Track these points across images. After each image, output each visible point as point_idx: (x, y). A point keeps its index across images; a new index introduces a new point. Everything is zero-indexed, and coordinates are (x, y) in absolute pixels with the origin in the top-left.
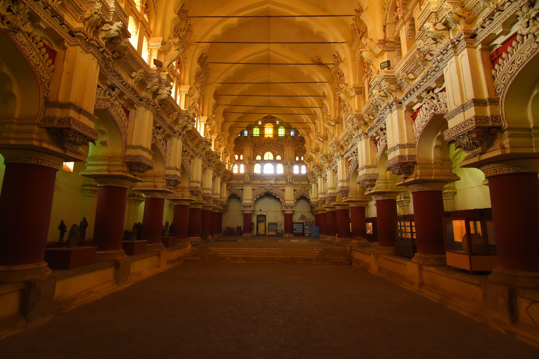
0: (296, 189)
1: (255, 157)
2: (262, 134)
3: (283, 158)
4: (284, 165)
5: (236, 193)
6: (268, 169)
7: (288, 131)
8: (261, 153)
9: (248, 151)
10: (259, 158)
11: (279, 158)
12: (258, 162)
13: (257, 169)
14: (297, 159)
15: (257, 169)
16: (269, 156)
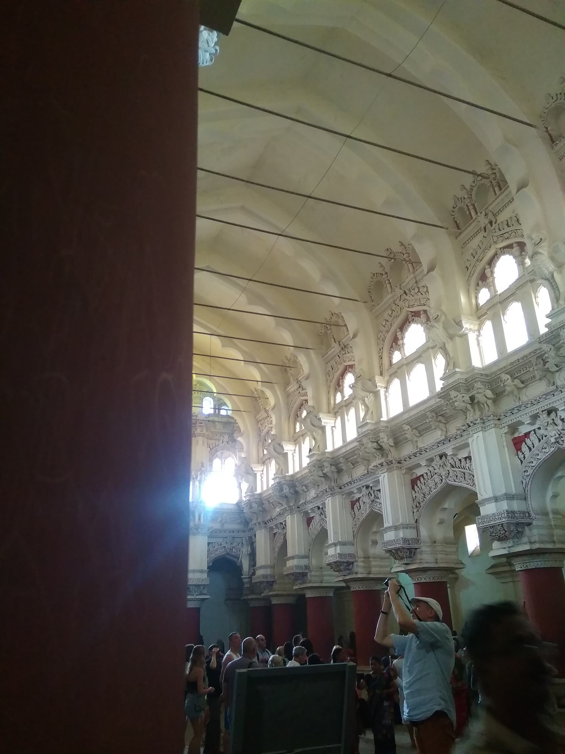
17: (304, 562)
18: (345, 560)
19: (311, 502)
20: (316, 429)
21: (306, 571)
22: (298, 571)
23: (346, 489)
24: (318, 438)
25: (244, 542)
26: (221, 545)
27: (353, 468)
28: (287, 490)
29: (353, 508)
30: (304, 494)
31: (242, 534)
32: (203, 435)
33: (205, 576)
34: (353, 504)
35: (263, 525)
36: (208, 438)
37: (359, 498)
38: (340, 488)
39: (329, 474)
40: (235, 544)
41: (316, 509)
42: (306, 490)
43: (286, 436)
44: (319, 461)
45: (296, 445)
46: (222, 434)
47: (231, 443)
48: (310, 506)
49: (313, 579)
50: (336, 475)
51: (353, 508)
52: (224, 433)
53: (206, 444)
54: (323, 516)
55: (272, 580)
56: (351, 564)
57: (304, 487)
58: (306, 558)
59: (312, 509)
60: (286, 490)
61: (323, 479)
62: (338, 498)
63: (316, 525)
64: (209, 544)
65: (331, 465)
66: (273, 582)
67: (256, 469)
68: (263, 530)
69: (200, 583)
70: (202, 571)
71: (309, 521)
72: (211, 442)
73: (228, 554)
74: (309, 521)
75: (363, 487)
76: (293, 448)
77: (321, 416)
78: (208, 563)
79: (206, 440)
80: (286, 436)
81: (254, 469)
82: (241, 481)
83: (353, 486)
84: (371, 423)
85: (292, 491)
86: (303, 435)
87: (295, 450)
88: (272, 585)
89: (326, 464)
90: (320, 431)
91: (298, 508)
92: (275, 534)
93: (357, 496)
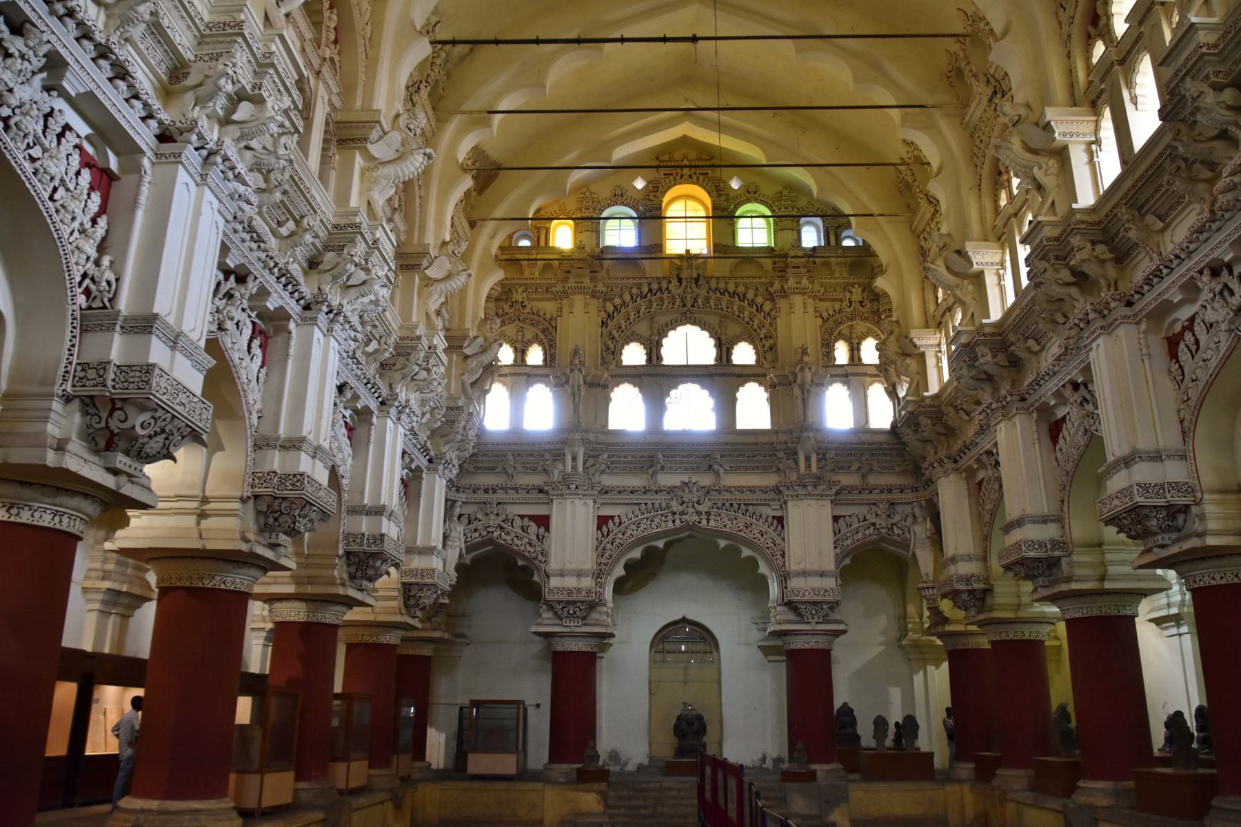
0: (838, 513)
1: (616, 354)
2: (652, 247)
3: (766, 350)
4: (771, 388)
5: (516, 539)
6: (691, 412)
7: (787, 223)
8: (643, 328)
9: (580, 322)
10: (634, 355)
11: (744, 354)
12: (634, 375)
13: (626, 411)
14: (841, 353)
15: (626, 411)
16: (689, 344)
17: (1049, 532)
18: (1160, 502)
19: (1051, 374)
20: (1042, 160)
21: (1057, 553)
22: (1031, 554)
23: (1149, 300)
24: (1049, 182)
25: (917, 512)
26: (865, 520)
27: (1162, 231)
28: (989, 358)
29: (1174, 355)
30: (1034, 359)
31: (909, 496)
32: (803, 291)
33: (830, 583)
34: (1173, 344)
35: (949, 465)
36: (814, 298)
37: (1192, 320)
38: (1130, 304)
39: (1091, 269)
40: (897, 518)
41: (1068, 392)
42: (1036, 348)
43: (975, 228)
44: (1057, 239)
45: (1003, 248)
46: (847, 287)
47: (869, 305)
48: (1052, 386)
49: (1078, 572)
50: (1111, 271)
51: (1174, 355)
52: (852, 285)
53: (811, 309)
54: (1090, 407)
55: (981, 586)
56: (1179, 511)
57: (1031, 343)
58: (1052, 521)
59: (1058, 394)
60: (986, 358)
61: (1074, 291)
62: (1127, 336)
63: (1071, 436)
64: (836, 519)
65: (1093, 243)
66: (984, 591)
67: (923, 342)
68: (951, 477)
69: (819, 598)
70: (822, 574)
71: (1055, 430)
72: (822, 305)
73: (882, 539)
74: (1055, 430)
75: (1201, 272)
76: (997, 258)
77: (1051, 114)
78: (839, 559)
79: (810, 301)
80: (975, 228)
81: (917, 342)
82: (895, 379)
83: (1167, 282)
84: (1210, 28)
85: (1002, 359)
86: (1016, 215)
87: (1002, 264)
88: (983, 599)
89: (1076, 241)
90: (1052, 163)
91: (1023, 399)
92: (980, 483)
93: (1185, 313)
